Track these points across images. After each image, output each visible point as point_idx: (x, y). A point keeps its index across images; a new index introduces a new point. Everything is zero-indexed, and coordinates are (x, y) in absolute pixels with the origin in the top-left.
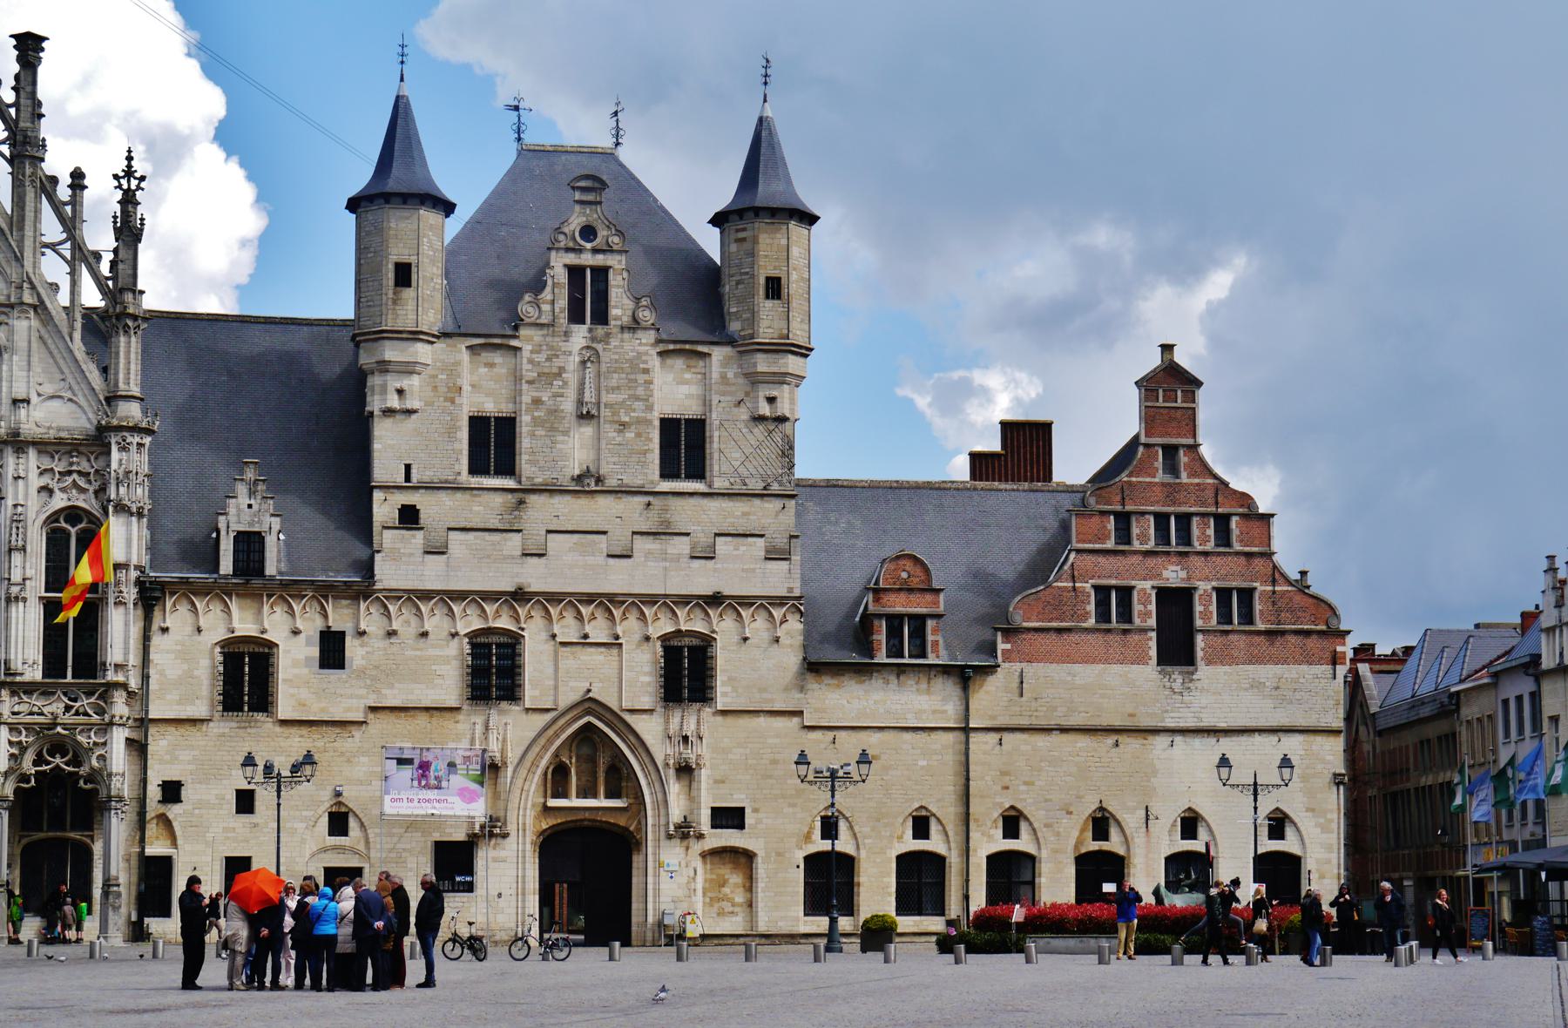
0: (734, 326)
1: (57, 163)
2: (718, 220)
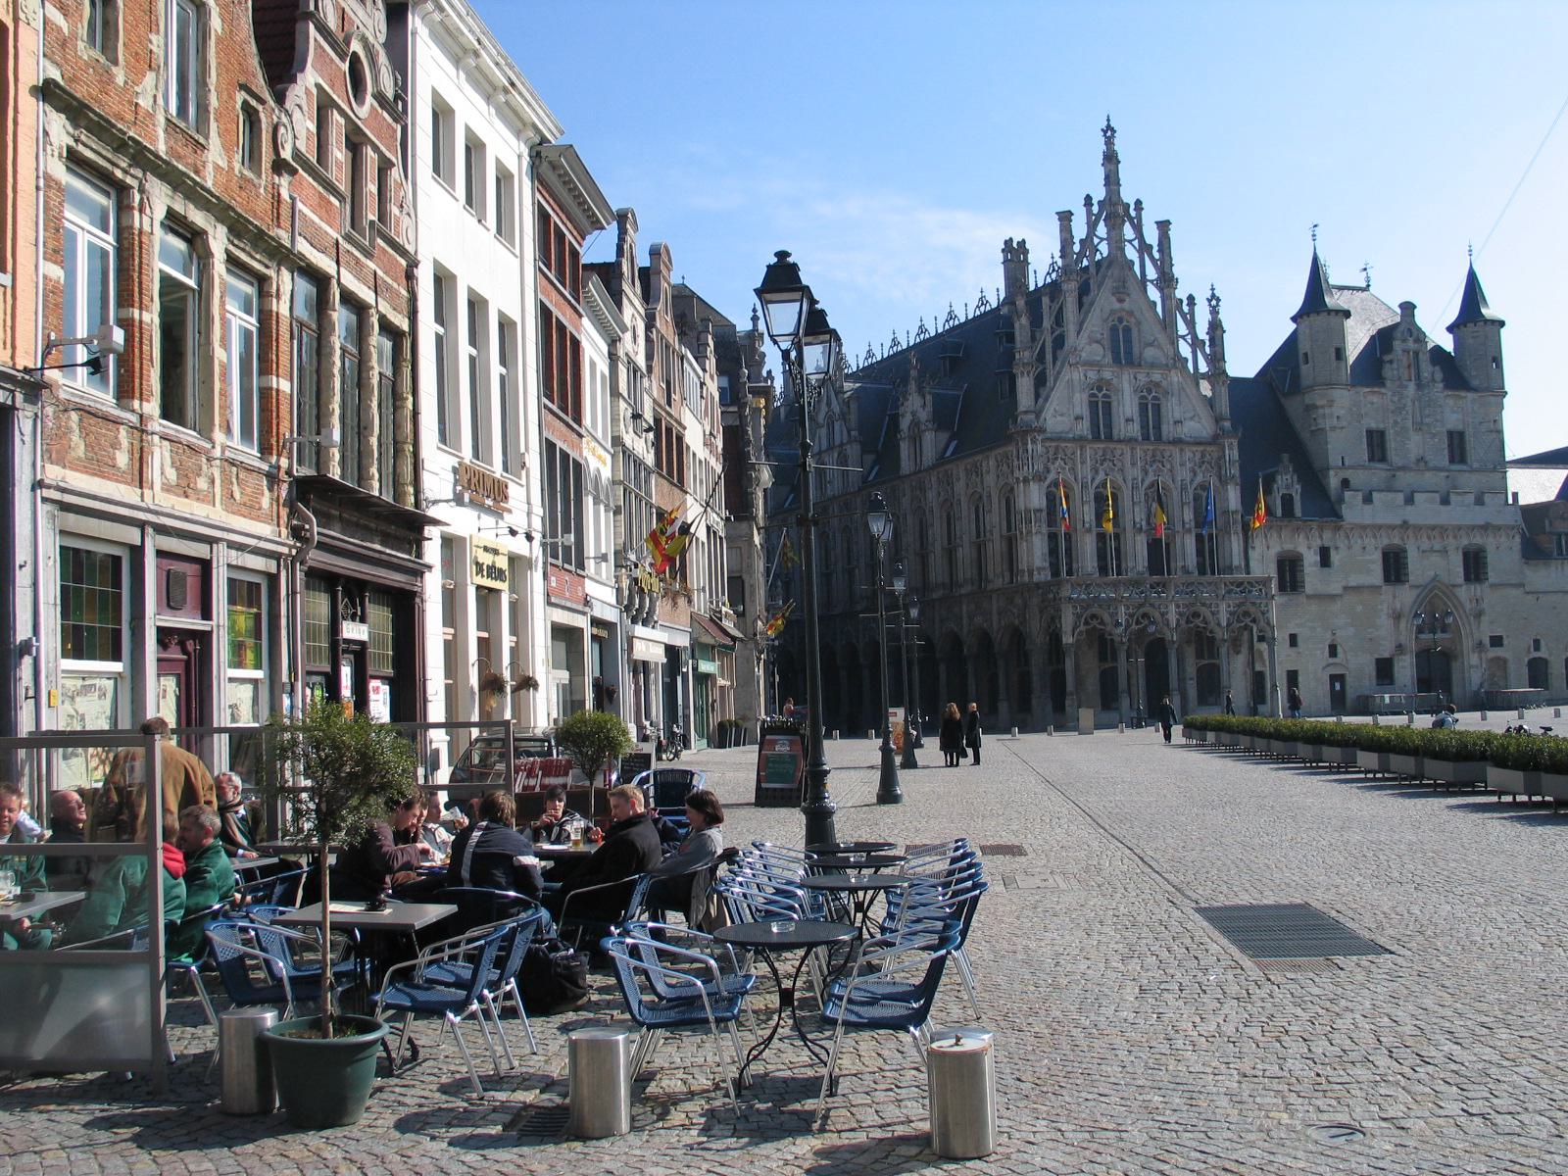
0: (1475, 383)
1: (1181, 293)
2: (1450, 329)
